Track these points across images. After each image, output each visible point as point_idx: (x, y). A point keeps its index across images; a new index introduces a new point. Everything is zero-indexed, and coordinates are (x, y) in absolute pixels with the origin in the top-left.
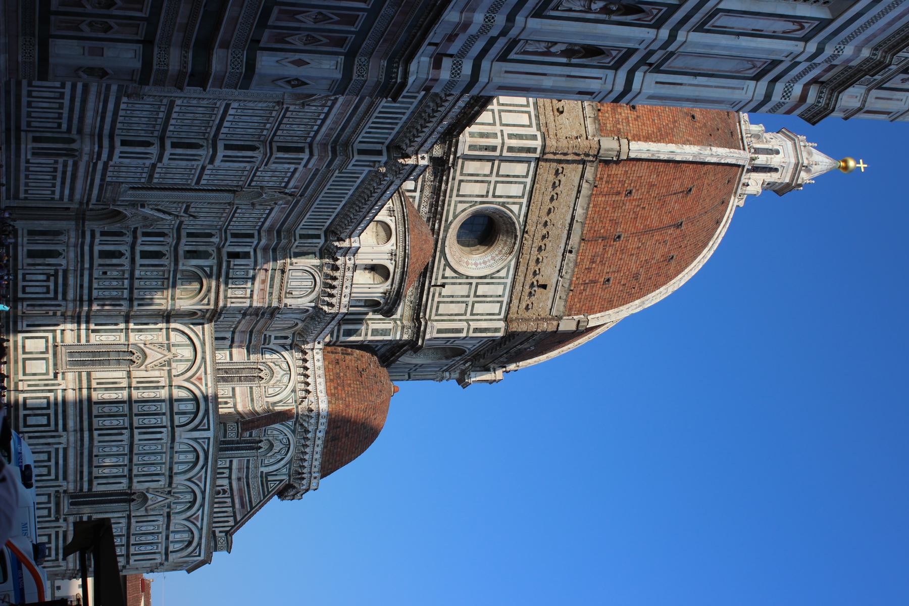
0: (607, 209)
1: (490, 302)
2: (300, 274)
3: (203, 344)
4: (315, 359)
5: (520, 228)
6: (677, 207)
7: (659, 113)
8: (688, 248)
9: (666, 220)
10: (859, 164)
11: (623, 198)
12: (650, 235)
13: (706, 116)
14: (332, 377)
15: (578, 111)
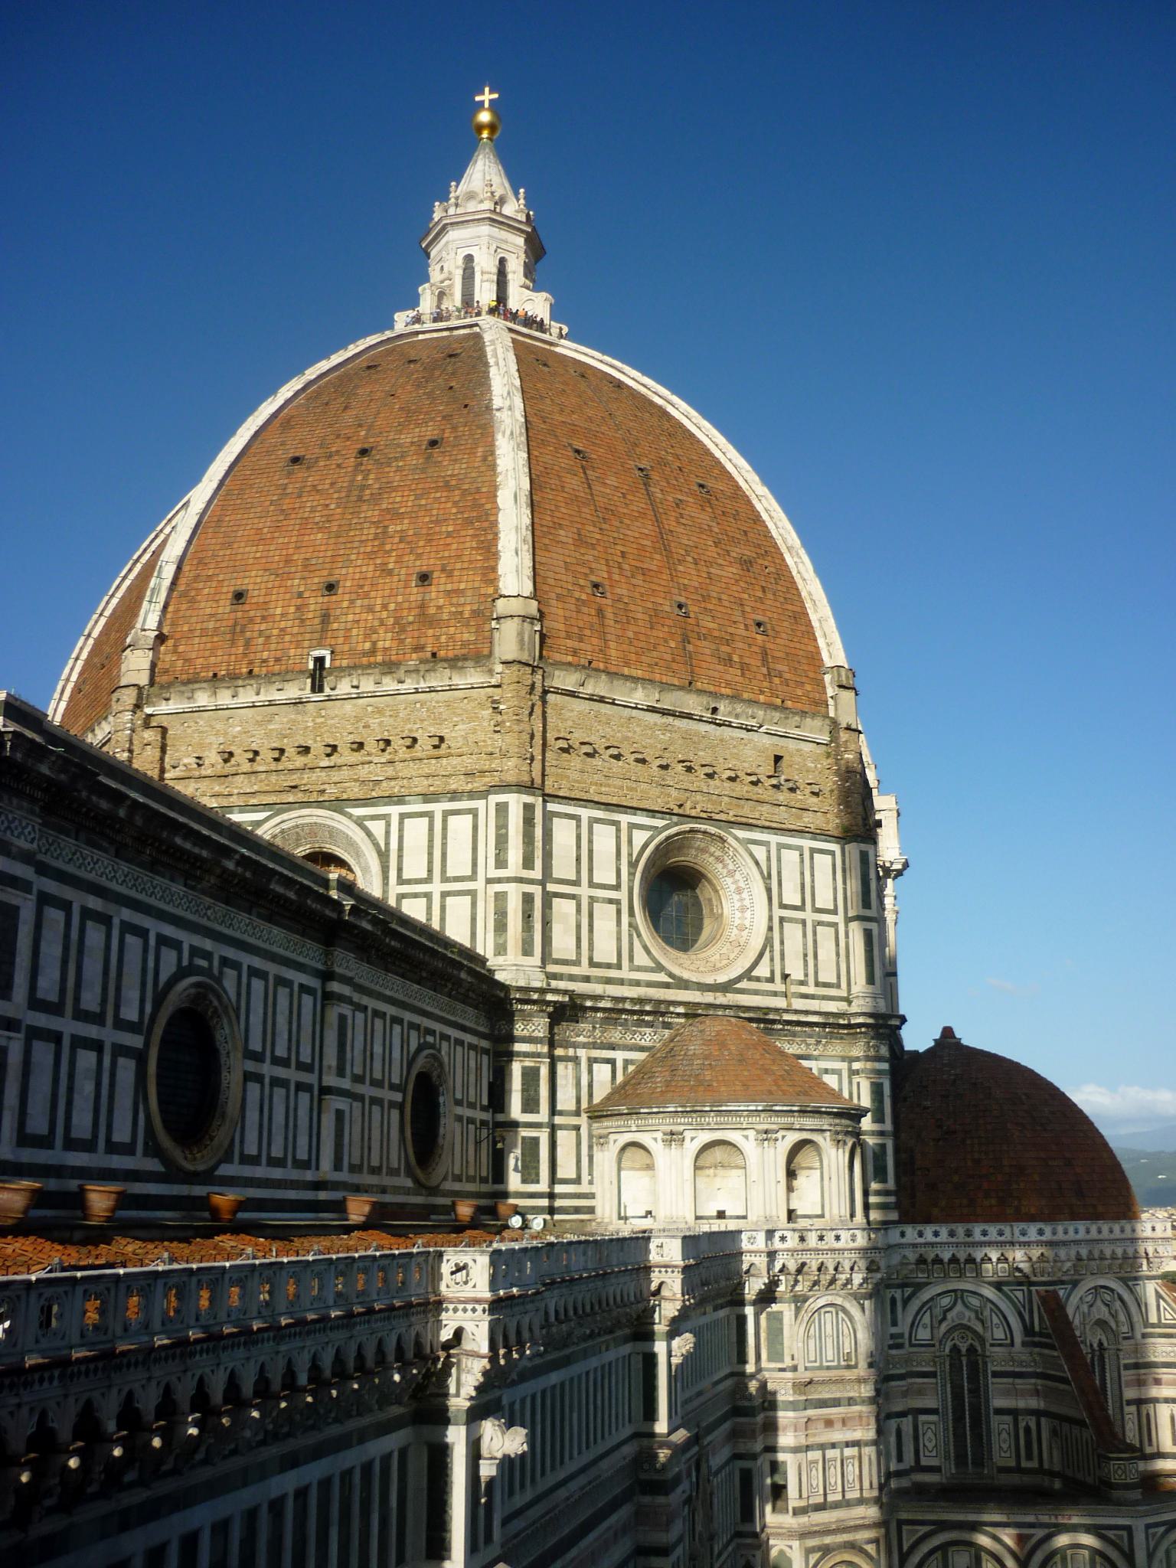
0: (630, 634)
1: (812, 875)
2: (812, 1342)
3: (943, 1526)
4: (935, 1240)
5: (676, 824)
6: (612, 481)
7: (431, 522)
8: (679, 452)
9: (639, 503)
10: (483, 102)
11: (609, 602)
12: (670, 538)
13: (427, 413)
14: (965, 1202)
15: (437, 702)
